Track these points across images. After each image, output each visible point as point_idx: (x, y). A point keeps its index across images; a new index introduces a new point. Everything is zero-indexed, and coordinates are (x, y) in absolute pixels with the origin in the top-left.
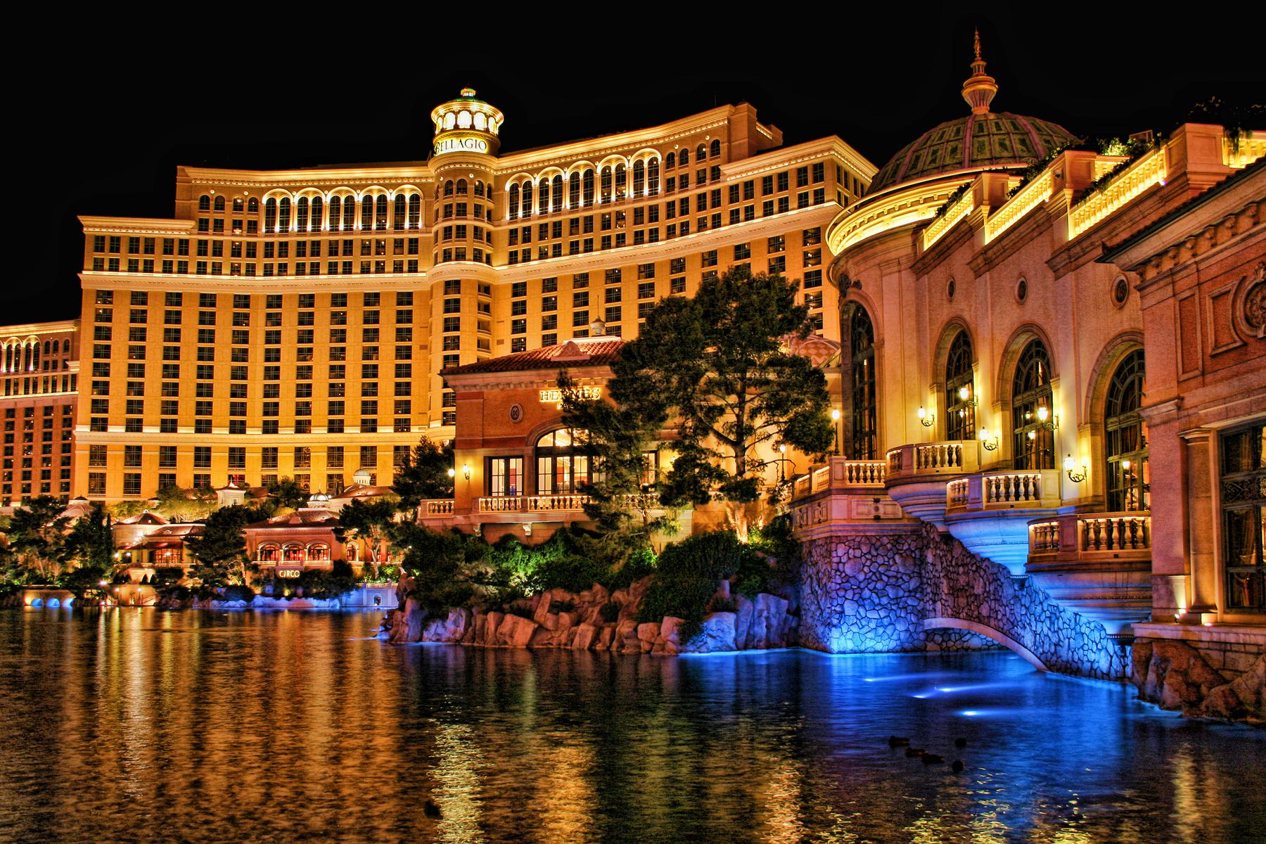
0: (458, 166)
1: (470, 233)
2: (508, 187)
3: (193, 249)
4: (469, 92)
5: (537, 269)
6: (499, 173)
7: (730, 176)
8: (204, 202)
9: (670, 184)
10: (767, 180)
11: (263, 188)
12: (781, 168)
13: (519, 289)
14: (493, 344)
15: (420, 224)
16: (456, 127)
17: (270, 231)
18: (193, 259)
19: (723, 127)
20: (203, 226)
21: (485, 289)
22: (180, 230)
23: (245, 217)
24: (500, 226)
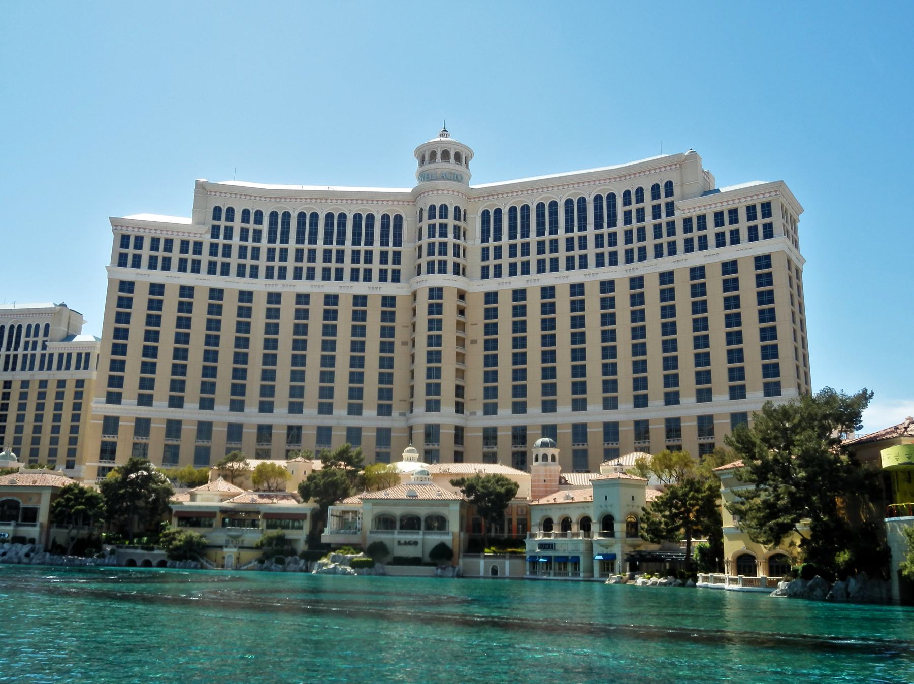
1: (450, 250)
3: (206, 249)
8: (217, 210)
9: (627, 215)
13: (491, 297)
14: (467, 342)
20: (215, 232)
21: (462, 296)
23: (251, 226)
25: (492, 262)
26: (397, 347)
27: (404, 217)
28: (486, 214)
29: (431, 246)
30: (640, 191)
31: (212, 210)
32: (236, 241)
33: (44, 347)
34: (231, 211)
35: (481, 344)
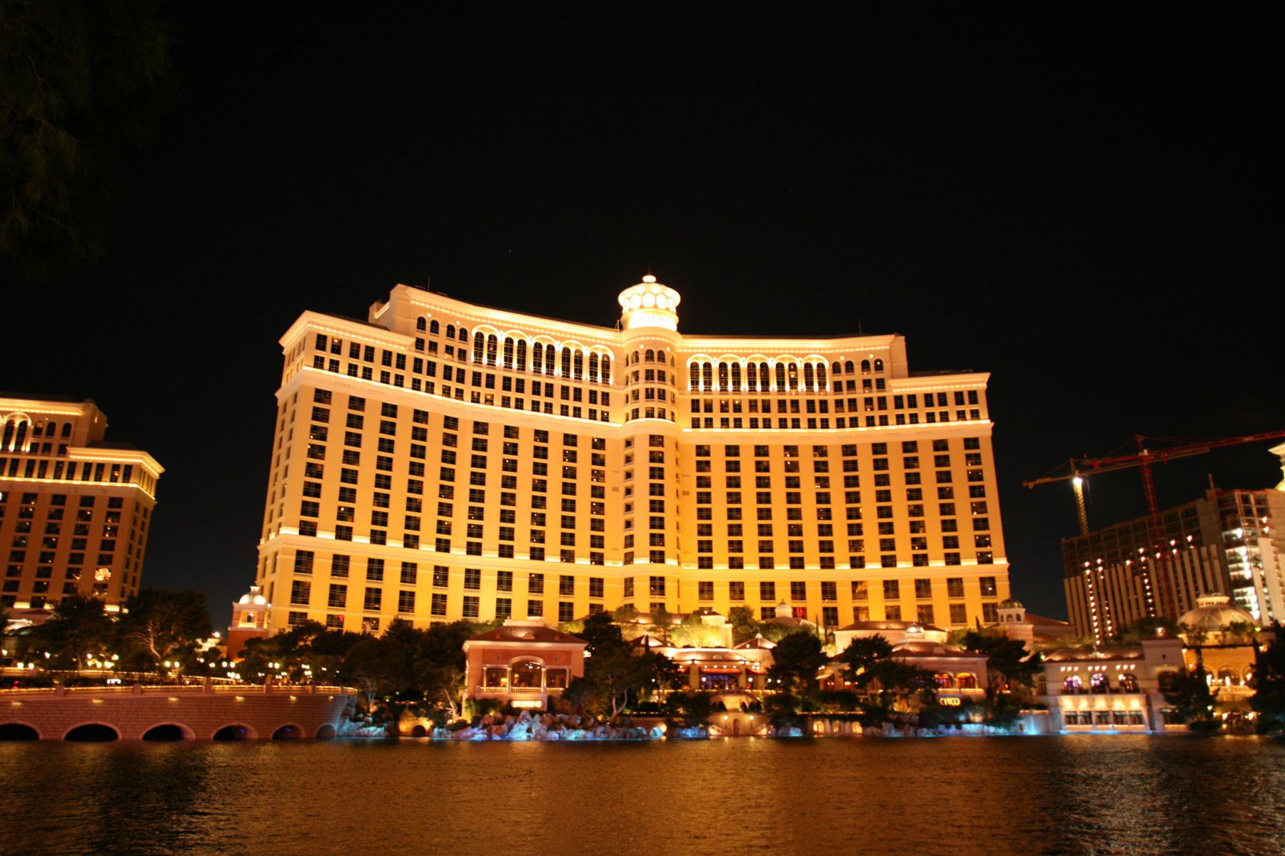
0: (658, 339)
1: (668, 396)
2: (689, 365)
3: (410, 364)
4: (649, 278)
5: (717, 436)
6: (680, 351)
7: (895, 388)
8: (421, 322)
9: (837, 387)
10: (928, 399)
11: (471, 322)
12: (941, 389)
13: (702, 450)
14: (680, 493)
15: (611, 380)
16: (656, 307)
17: (478, 362)
18: (408, 374)
19: (885, 350)
20: (419, 344)
22: (400, 345)
23: (457, 344)
24: (683, 394)
25: (702, 415)
26: (607, 493)
27: (612, 358)
28: (694, 367)
29: (649, 394)
30: (849, 366)
31: (416, 321)
32: (442, 360)
33: (63, 451)
34: (435, 327)
35: (694, 497)
